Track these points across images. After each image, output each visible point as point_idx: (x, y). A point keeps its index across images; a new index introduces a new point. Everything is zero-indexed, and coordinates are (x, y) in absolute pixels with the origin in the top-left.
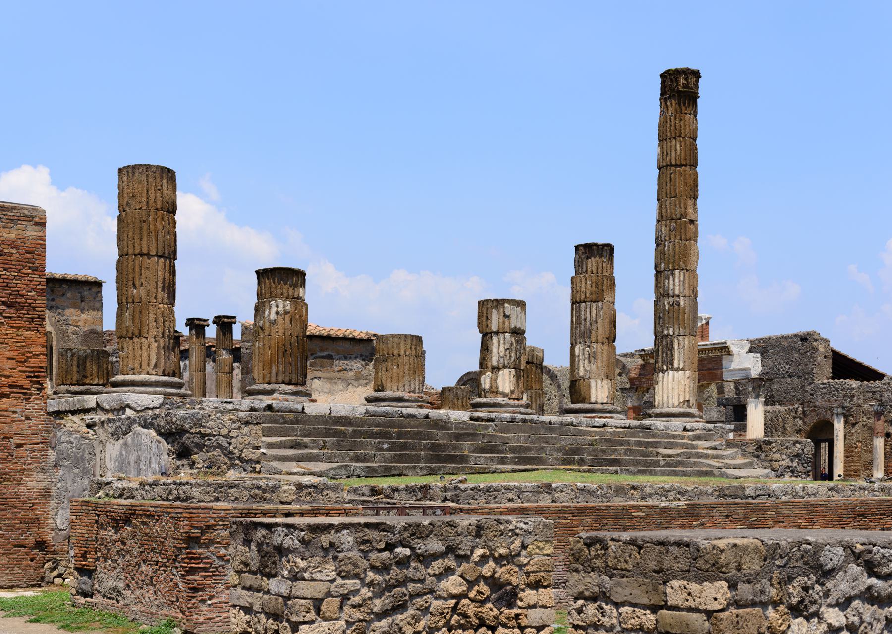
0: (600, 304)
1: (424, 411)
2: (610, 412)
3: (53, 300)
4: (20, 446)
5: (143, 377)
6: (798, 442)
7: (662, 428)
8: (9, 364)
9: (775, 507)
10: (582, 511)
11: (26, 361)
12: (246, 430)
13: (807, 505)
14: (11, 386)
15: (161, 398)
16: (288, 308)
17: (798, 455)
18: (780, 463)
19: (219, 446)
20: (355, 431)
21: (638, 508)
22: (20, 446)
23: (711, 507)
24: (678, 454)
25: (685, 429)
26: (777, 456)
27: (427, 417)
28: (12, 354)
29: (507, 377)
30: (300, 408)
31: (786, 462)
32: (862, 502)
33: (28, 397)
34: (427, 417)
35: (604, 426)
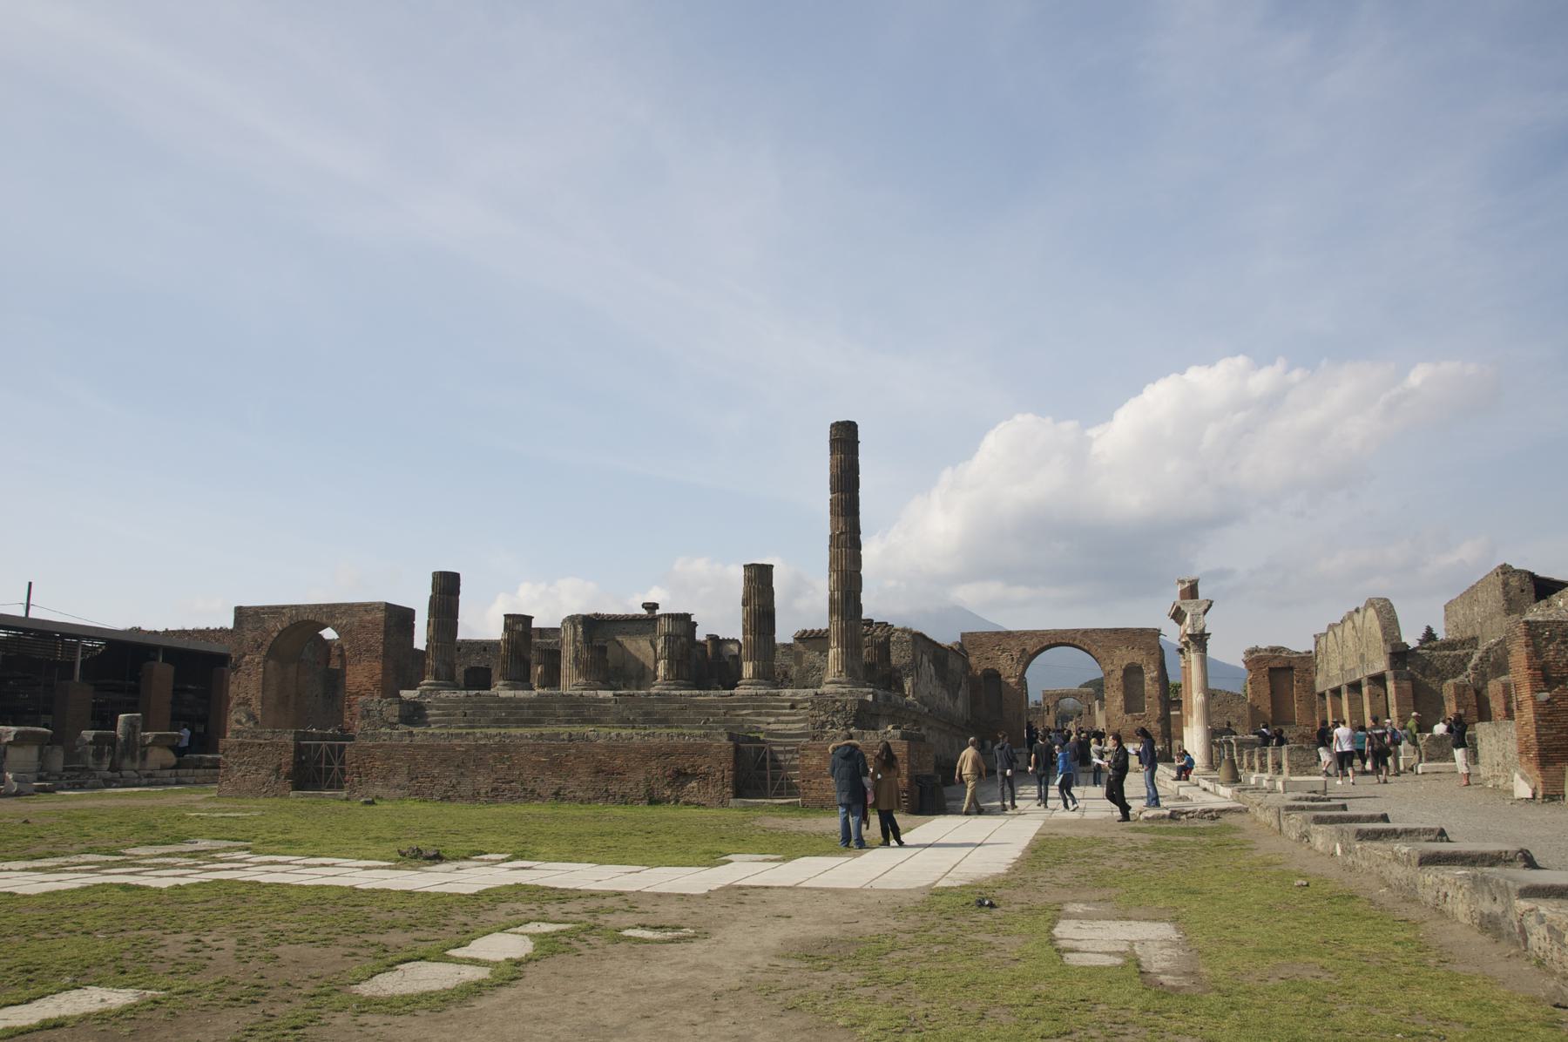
13: (607, 747)
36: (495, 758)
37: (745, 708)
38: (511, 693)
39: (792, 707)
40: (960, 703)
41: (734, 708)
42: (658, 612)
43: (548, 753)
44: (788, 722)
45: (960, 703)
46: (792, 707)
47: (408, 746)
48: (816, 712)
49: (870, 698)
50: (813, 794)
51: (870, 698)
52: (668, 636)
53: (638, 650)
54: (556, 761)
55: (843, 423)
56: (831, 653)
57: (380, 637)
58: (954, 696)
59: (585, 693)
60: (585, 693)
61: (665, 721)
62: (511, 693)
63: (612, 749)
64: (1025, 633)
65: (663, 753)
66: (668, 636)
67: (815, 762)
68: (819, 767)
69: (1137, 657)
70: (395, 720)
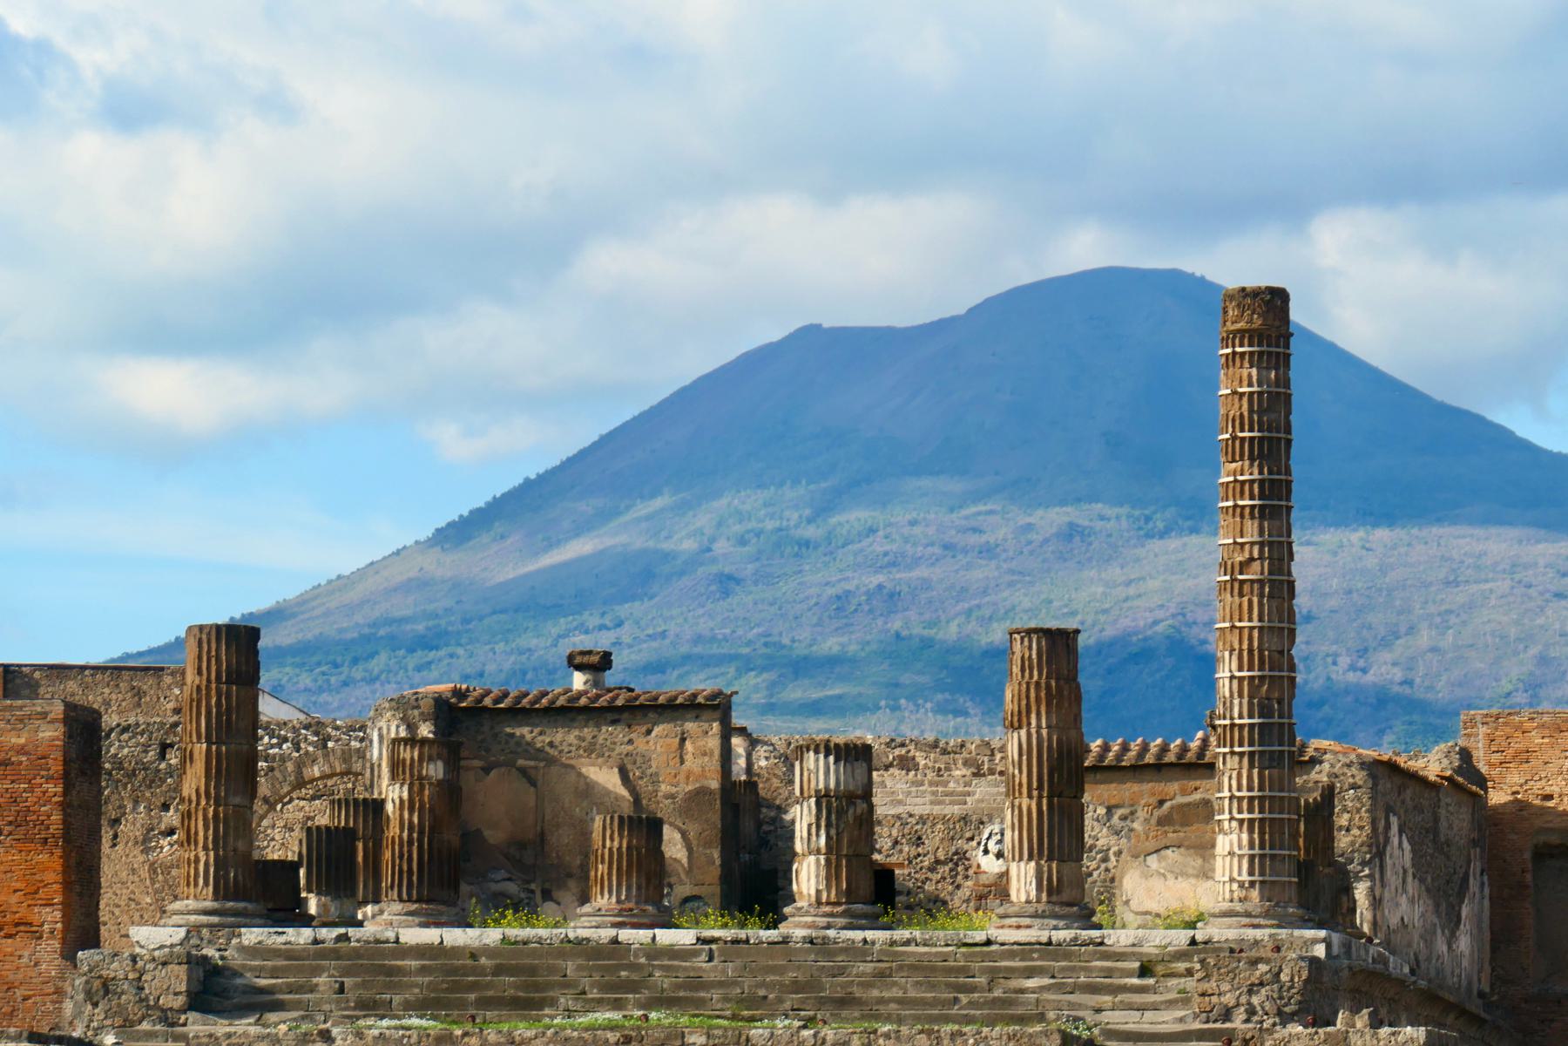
0: (1023, 732)
1: (612, 932)
3: (630, 742)
4: (25, 999)
5: (191, 904)
7: (1130, 941)
8: (14, 899)
11: (36, 892)
14: (17, 925)
15: (182, 932)
16: (405, 795)
18: (1214, 999)
20: (423, 968)
22: (25, 999)
24: (1042, 989)
25: (1193, 942)
26: (1211, 986)
27: (615, 941)
28: (18, 885)
29: (813, 868)
30: (391, 935)
34: (615, 941)
35: (989, 943)
37: (1030, 973)
38: (430, 935)
39: (1144, 971)
40: (1464, 943)
41: (1010, 973)
42: (611, 678)
44: (1142, 1008)
45: (1464, 943)
46: (1144, 971)
48: (1211, 986)
49: (1320, 951)
51: (1320, 951)
52: (822, 798)
55: (1256, 293)
56: (1223, 843)
57: (55, 789)
58: (1453, 922)
59: (626, 935)
60: (626, 935)
62: (430, 935)
66: (822, 798)
70: (180, 1001)
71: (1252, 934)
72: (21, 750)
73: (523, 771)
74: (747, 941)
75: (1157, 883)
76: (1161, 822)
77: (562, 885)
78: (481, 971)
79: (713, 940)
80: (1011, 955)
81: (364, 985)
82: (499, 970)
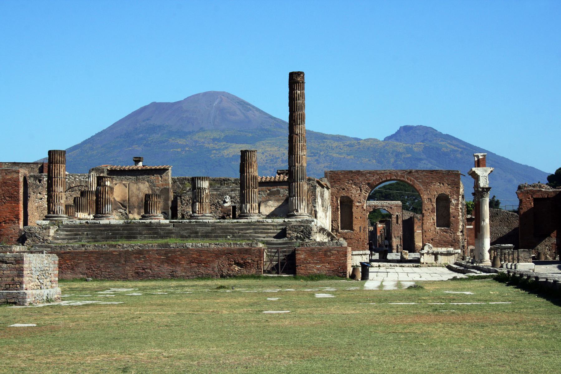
1: (150, 221)
2: (247, 216)
6: (302, 226)
9: (180, 250)
10: (92, 252)
12: (44, 231)
17: (302, 232)
19: (35, 236)
21: (114, 251)
23: (148, 251)
24: (251, 233)
25: (284, 221)
26: (289, 232)
27: (151, 222)
30: (98, 222)
31: (295, 234)
32: (228, 249)
33: (14, 223)
34: (151, 222)
35: (237, 222)
36: (135, 258)
43: (166, 254)
47: (85, 252)
50: (302, 272)
53: (139, 189)
54: (170, 257)
59: (153, 221)
61: (206, 236)
63: (200, 252)
64: (370, 173)
65: (229, 253)
67: (303, 257)
68: (305, 259)
69: (445, 189)
71: (298, 220)
72: (10, 180)
73: (124, 184)
74: (181, 222)
75: (268, 208)
76: (268, 194)
77: (133, 209)
78: (119, 230)
79: (173, 222)
80: (243, 225)
81: (92, 234)
82: (123, 230)
